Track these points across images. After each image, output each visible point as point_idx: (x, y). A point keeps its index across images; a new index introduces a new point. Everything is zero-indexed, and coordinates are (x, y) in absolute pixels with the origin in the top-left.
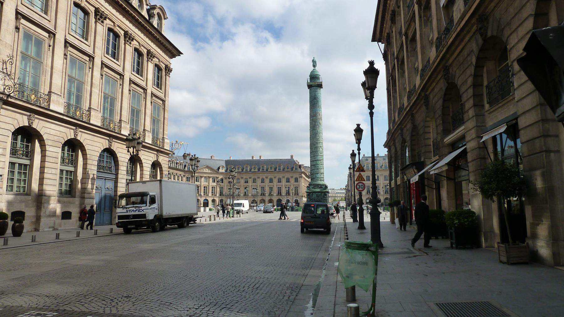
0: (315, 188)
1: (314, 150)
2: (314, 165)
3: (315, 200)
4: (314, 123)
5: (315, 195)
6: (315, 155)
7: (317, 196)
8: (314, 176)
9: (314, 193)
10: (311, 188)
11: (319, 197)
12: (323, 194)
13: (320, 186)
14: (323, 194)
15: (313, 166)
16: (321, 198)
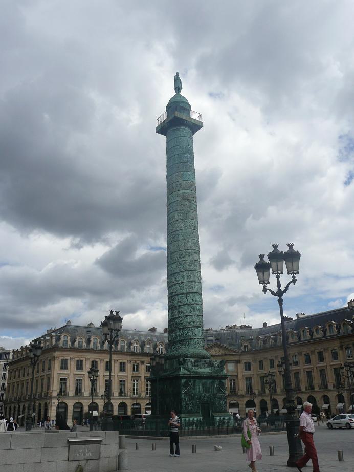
0: (197, 366)
1: (190, 266)
2: (189, 304)
3: (200, 399)
4: (187, 203)
5: (201, 386)
6: (192, 279)
7: (206, 390)
8: (190, 334)
9: (197, 381)
10: (189, 365)
11: (209, 392)
12: (217, 383)
13: (208, 361)
14: (217, 383)
15: (186, 307)
16: (214, 395)
